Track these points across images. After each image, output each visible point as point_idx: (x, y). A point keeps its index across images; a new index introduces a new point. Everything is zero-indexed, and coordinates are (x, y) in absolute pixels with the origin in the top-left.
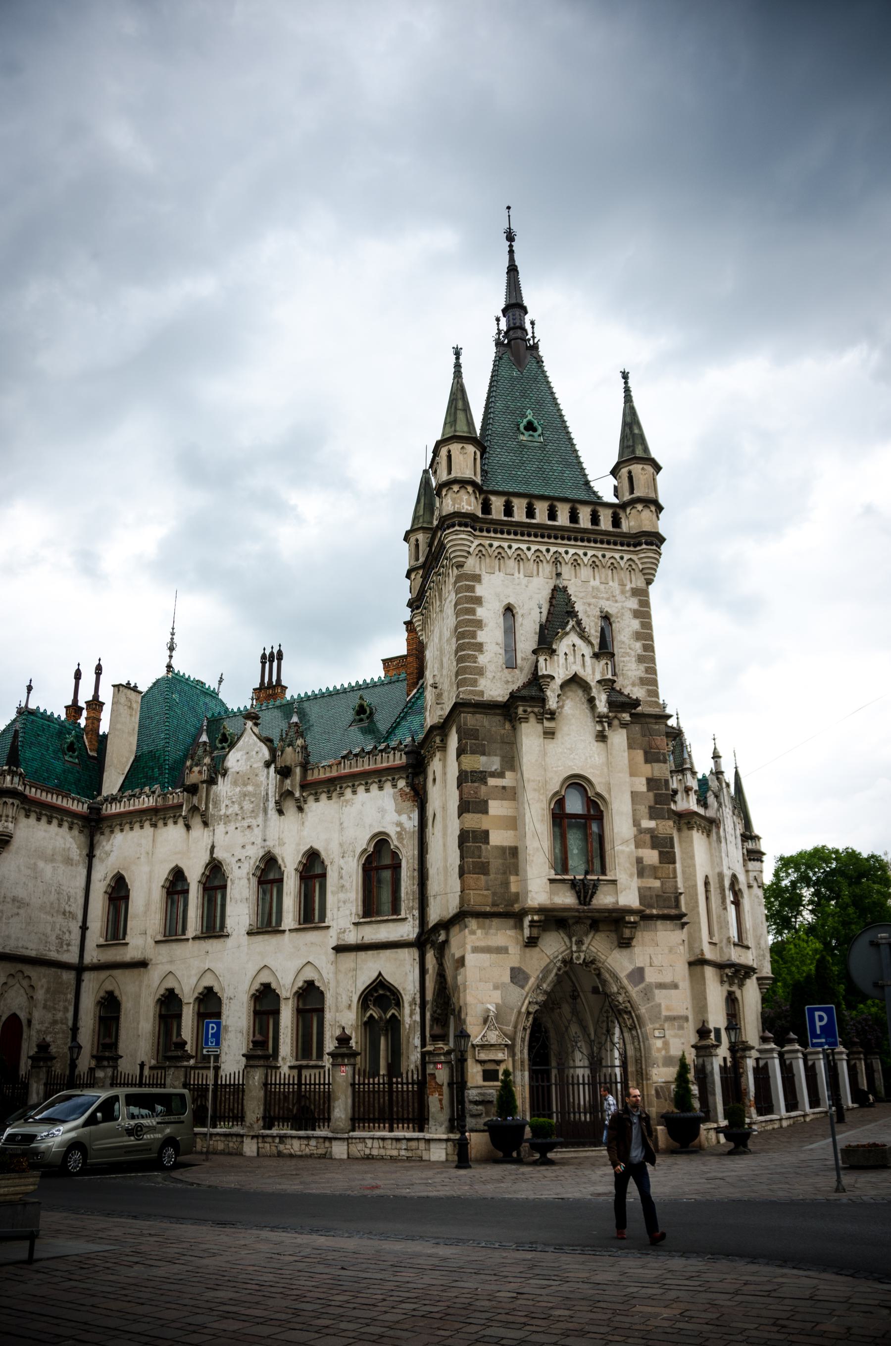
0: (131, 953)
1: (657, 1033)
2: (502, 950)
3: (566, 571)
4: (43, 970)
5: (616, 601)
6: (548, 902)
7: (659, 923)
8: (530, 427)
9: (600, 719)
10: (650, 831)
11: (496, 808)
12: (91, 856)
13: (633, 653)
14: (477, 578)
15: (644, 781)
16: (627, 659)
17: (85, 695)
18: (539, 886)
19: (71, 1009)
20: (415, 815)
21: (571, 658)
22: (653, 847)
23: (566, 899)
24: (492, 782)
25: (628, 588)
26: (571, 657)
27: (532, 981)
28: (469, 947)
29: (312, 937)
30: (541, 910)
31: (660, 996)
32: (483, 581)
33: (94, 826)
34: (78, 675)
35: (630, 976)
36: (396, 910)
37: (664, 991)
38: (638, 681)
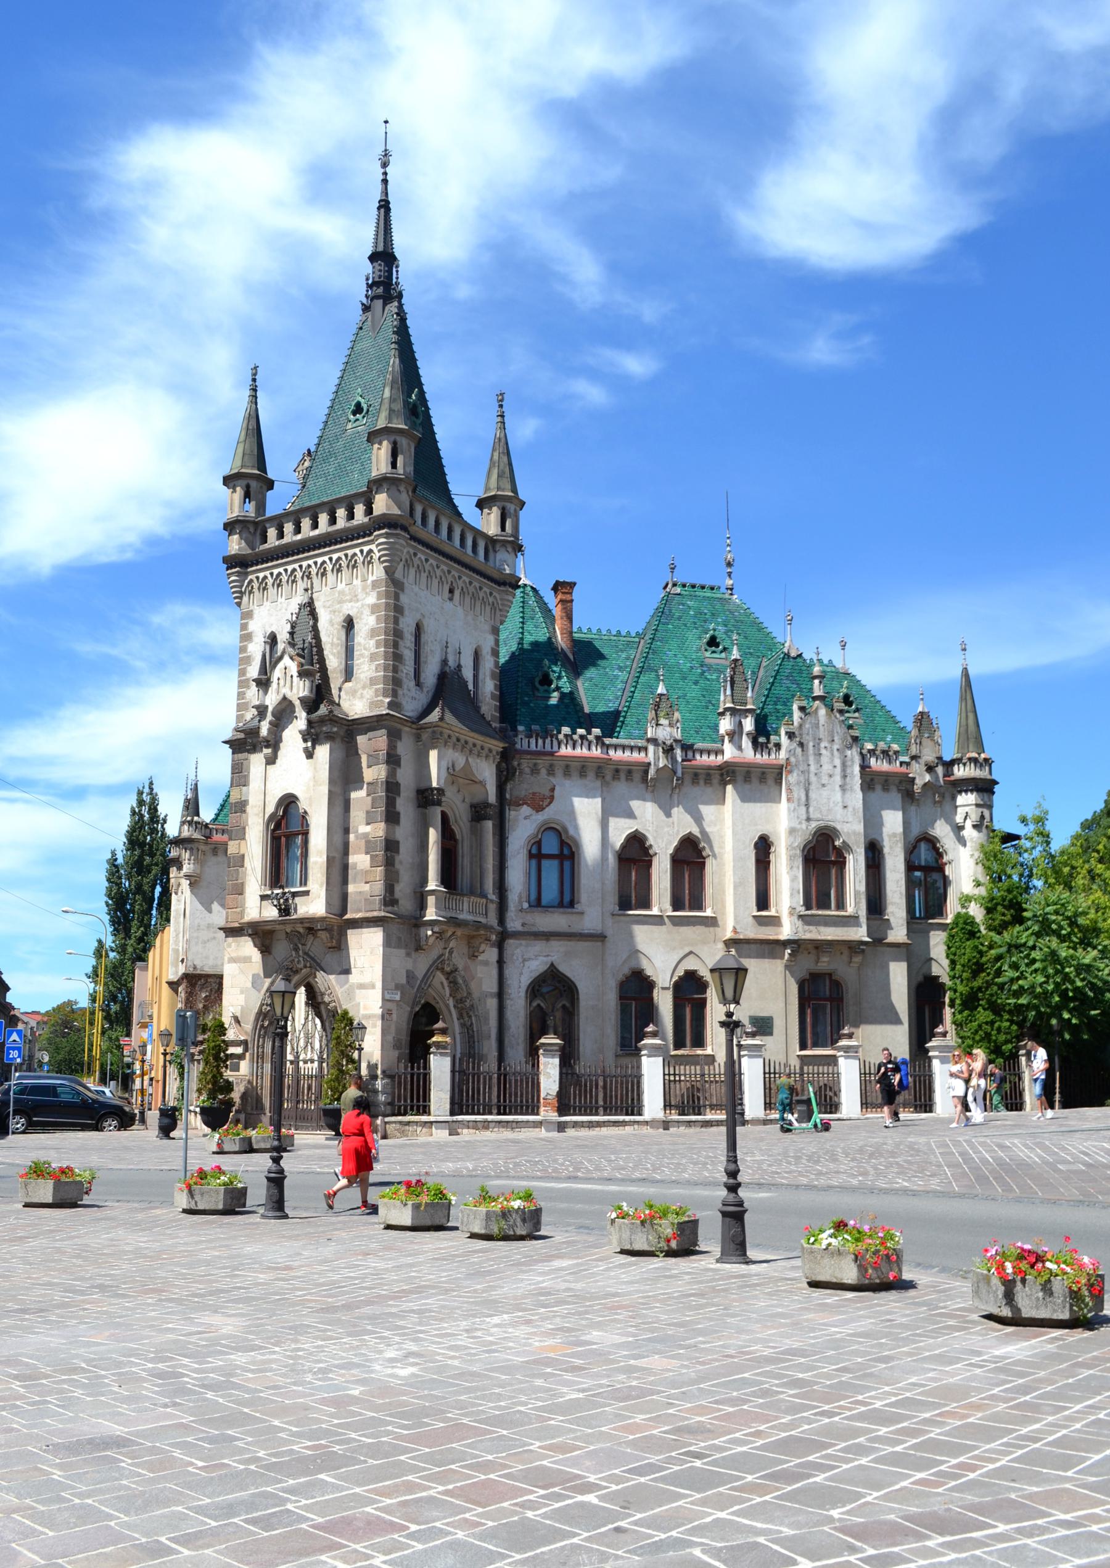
2: (247, 960)
5: (358, 601)
13: (367, 653)
21: (282, 682)
25: (369, 582)
28: (226, 959)
32: (255, 616)
37: (363, 991)
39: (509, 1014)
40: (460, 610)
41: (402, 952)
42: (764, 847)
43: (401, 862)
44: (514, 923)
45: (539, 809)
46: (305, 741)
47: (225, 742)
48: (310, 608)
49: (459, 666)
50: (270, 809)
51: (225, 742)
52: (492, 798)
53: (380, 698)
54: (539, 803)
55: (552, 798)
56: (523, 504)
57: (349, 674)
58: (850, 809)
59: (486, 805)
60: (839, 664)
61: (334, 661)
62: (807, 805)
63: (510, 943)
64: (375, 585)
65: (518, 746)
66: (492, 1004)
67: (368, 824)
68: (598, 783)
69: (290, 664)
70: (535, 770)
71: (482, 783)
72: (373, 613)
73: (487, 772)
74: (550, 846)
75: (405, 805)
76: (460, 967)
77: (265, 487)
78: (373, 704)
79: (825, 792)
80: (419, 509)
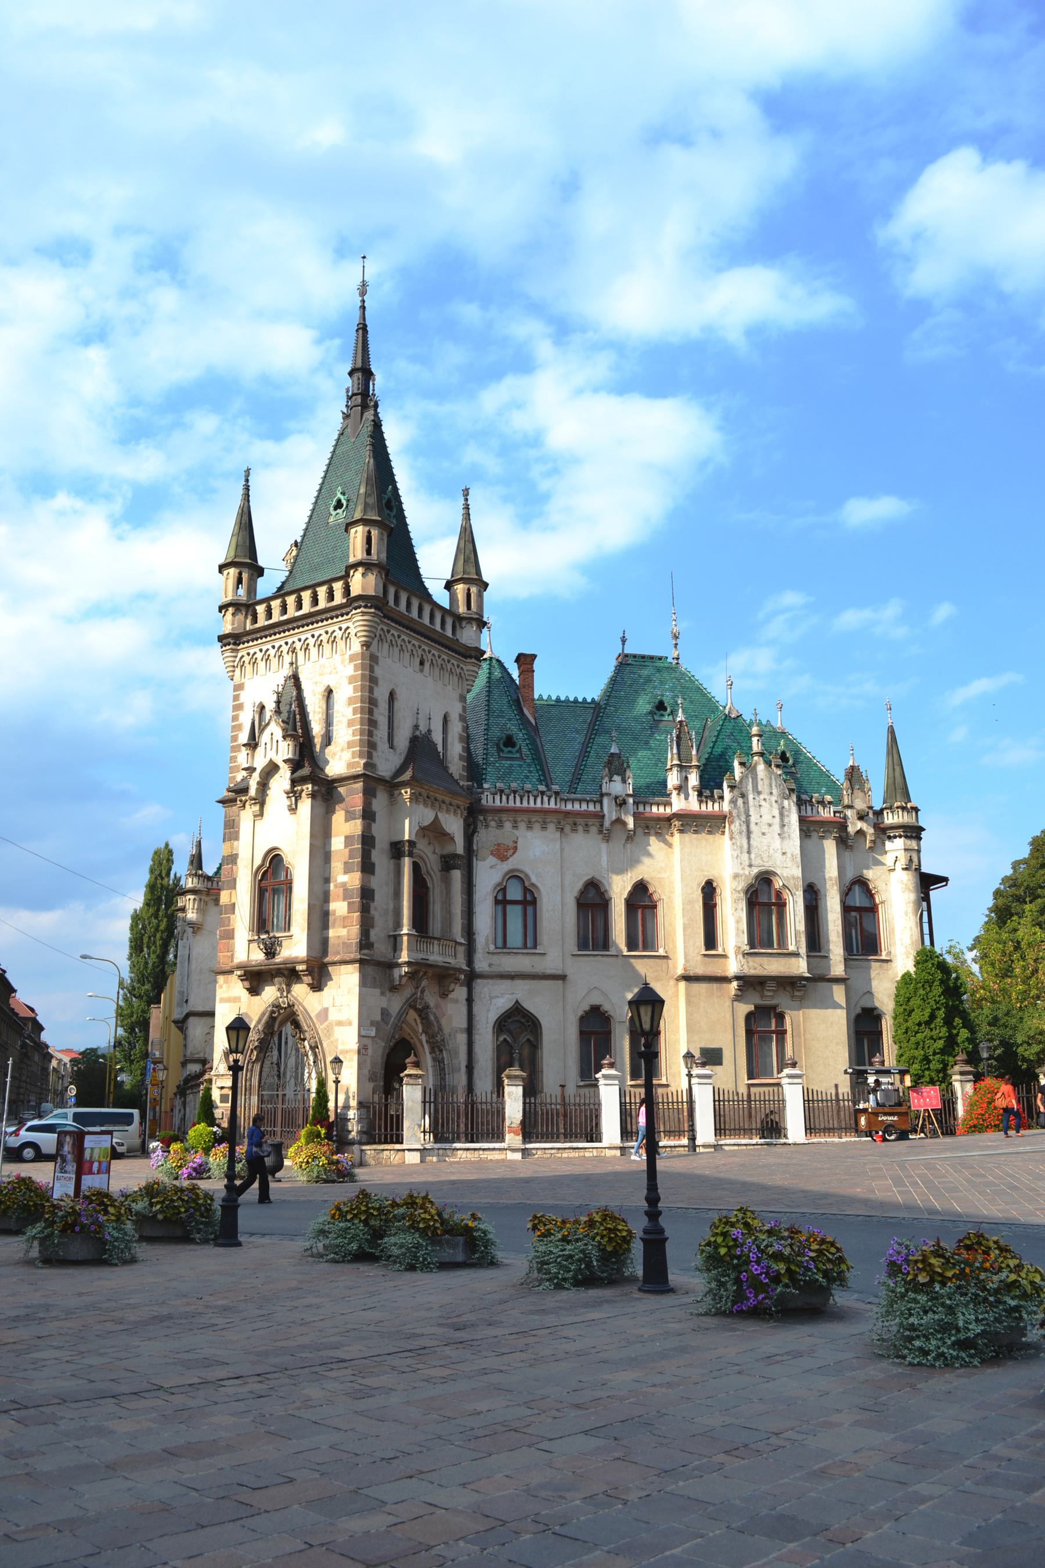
2: (236, 1000)
7: (343, 967)
8: (339, 505)
10: (344, 884)
15: (343, 839)
21: (268, 746)
22: (344, 900)
25: (347, 657)
35: (318, 1015)
39: (478, 1049)
40: (430, 679)
41: (377, 991)
42: (709, 891)
43: (376, 909)
44: (481, 964)
45: (503, 858)
47: (219, 802)
48: (295, 679)
49: (429, 731)
50: (258, 862)
51: (219, 802)
52: (460, 849)
53: (357, 759)
54: (502, 853)
55: (515, 848)
56: (486, 585)
57: (328, 740)
58: (789, 855)
59: (455, 856)
60: (778, 724)
61: (317, 728)
62: (749, 852)
63: (479, 984)
64: (352, 658)
65: (484, 802)
66: (462, 1039)
67: (345, 873)
68: (558, 834)
69: (275, 730)
70: (500, 825)
71: (450, 838)
72: (350, 683)
73: (454, 825)
74: (515, 893)
75: (380, 857)
76: (432, 1005)
77: (255, 574)
78: (350, 765)
79: (765, 840)
80: (392, 590)
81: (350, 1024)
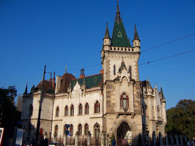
0: (60, 118)
1: (137, 132)
2: (113, 119)
3: (124, 59)
4: (46, 121)
6: (119, 112)
9: (128, 83)
10: (137, 100)
11: (112, 97)
12: (53, 103)
14: (109, 61)
16: (134, 73)
17: (52, 77)
18: (118, 109)
19: (51, 127)
20: (102, 97)
21: (124, 73)
22: (137, 103)
23: (123, 111)
24: (111, 93)
26: (125, 73)
27: (117, 124)
29: (87, 116)
30: (118, 113)
31: (138, 126)
33: (54, 98)
34: (51, 74)
36: (99, 112)
37: (138, 126)
38: (135, 76)
46: (128, 83)
64: (135, 62)
67: (137, 98)
81: (140, 125)
